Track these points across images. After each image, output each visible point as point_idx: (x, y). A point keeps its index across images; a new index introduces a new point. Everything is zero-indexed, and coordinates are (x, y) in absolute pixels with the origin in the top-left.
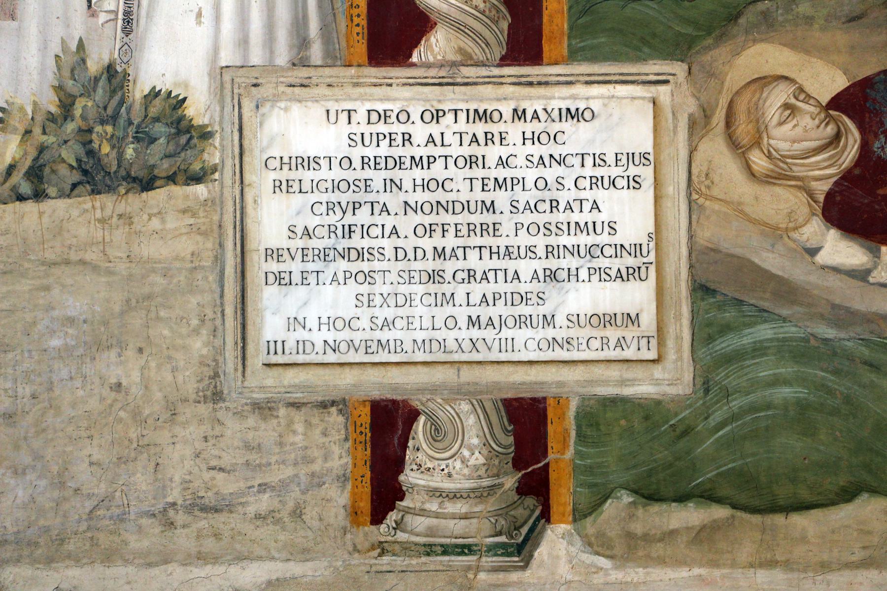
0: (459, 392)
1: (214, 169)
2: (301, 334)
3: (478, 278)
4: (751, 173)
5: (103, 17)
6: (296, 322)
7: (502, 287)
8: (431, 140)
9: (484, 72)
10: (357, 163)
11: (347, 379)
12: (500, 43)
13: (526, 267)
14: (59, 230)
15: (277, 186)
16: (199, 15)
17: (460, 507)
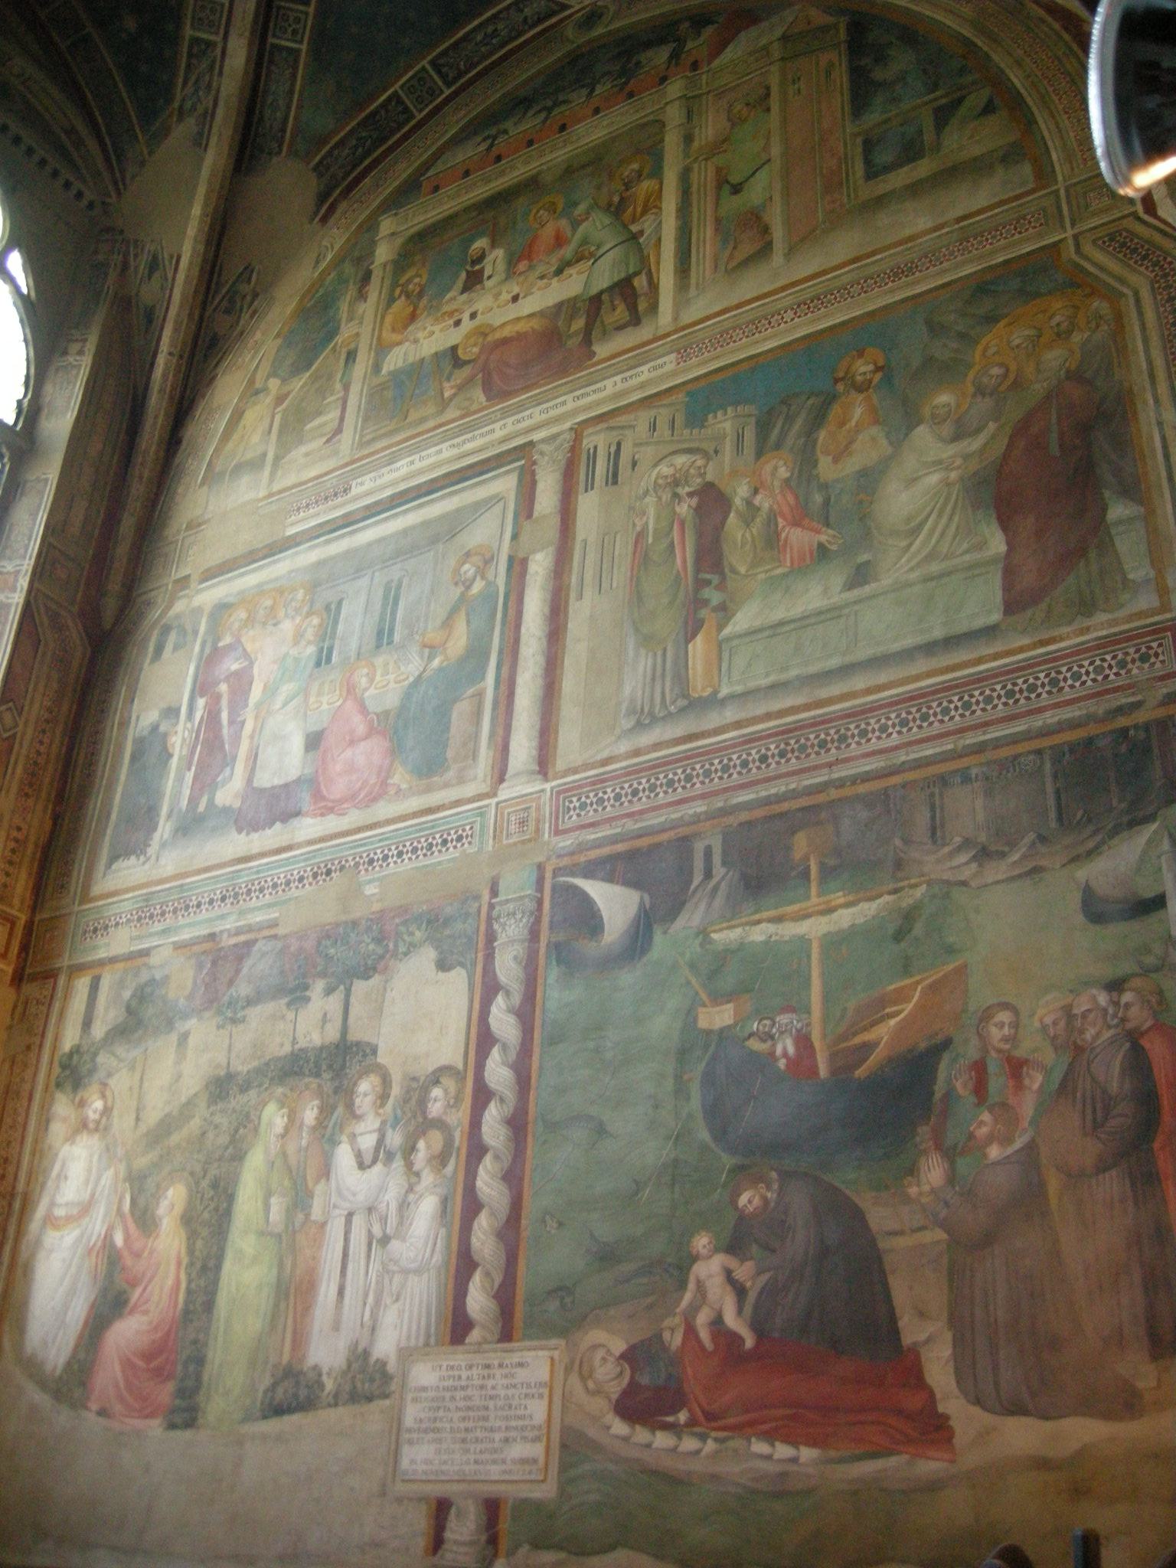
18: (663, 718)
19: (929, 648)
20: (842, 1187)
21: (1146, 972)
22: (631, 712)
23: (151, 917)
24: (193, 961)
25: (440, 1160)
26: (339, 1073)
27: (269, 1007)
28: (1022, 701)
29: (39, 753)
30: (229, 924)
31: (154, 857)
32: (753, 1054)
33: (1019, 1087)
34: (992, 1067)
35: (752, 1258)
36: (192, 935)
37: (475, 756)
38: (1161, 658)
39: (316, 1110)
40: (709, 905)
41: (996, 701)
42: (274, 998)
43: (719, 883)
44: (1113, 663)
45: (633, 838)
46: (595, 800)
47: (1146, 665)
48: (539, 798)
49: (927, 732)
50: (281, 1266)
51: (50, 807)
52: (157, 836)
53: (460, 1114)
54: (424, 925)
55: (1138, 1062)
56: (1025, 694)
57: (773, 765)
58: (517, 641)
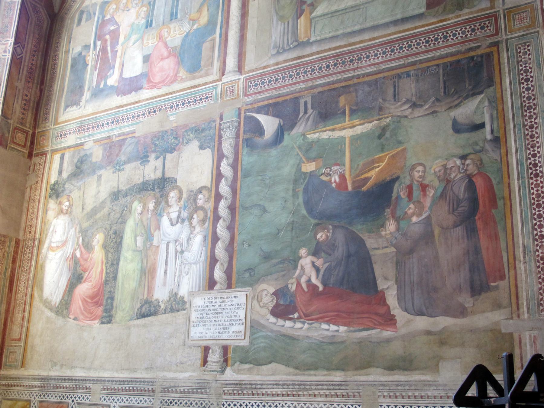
0: (217, 345)
2: (196, 335)
4: (260, 306)
6: (195, 333)
7: (223, 327)
8: (215, 302)
9: (223, 290)
11: (201, 342)
13: (227, 323)
17: (215, 364)
18: (288, 49)
19: (395, 23)
20: (356, 232)
21: (476, 152)
22: (275, 47)
23: (84, 130)
24: (102, 147)
25: (203, 221)
26: (162, 189)
27: (133, 165)
28: (432, 45)
29: (32, 64)
30: (116, 132)
31: (83, 106)
32: (322, 181)
33: (425, 195)
34: (415, 188)
35: (322, 258)
36: (101, 137)
37: (212, 64)
38: (489, 28)
39: (153, 204)
40: (306, 124)
41: (421, 45)
42: (135, 161)
43: (310, 115)
44: (470, 30)
45: (276, 98)
46: (261, 83)
47: (483, 31)
48: (238, 82)
49: (393, 57)
50: (142, 262)
51: (39, 86)
52: (84, 97)
53: (210, 204)
54: (194, 132)
55: (471, 186)
56: (433, 42)
57: (332, 69)
58: (228, 18)
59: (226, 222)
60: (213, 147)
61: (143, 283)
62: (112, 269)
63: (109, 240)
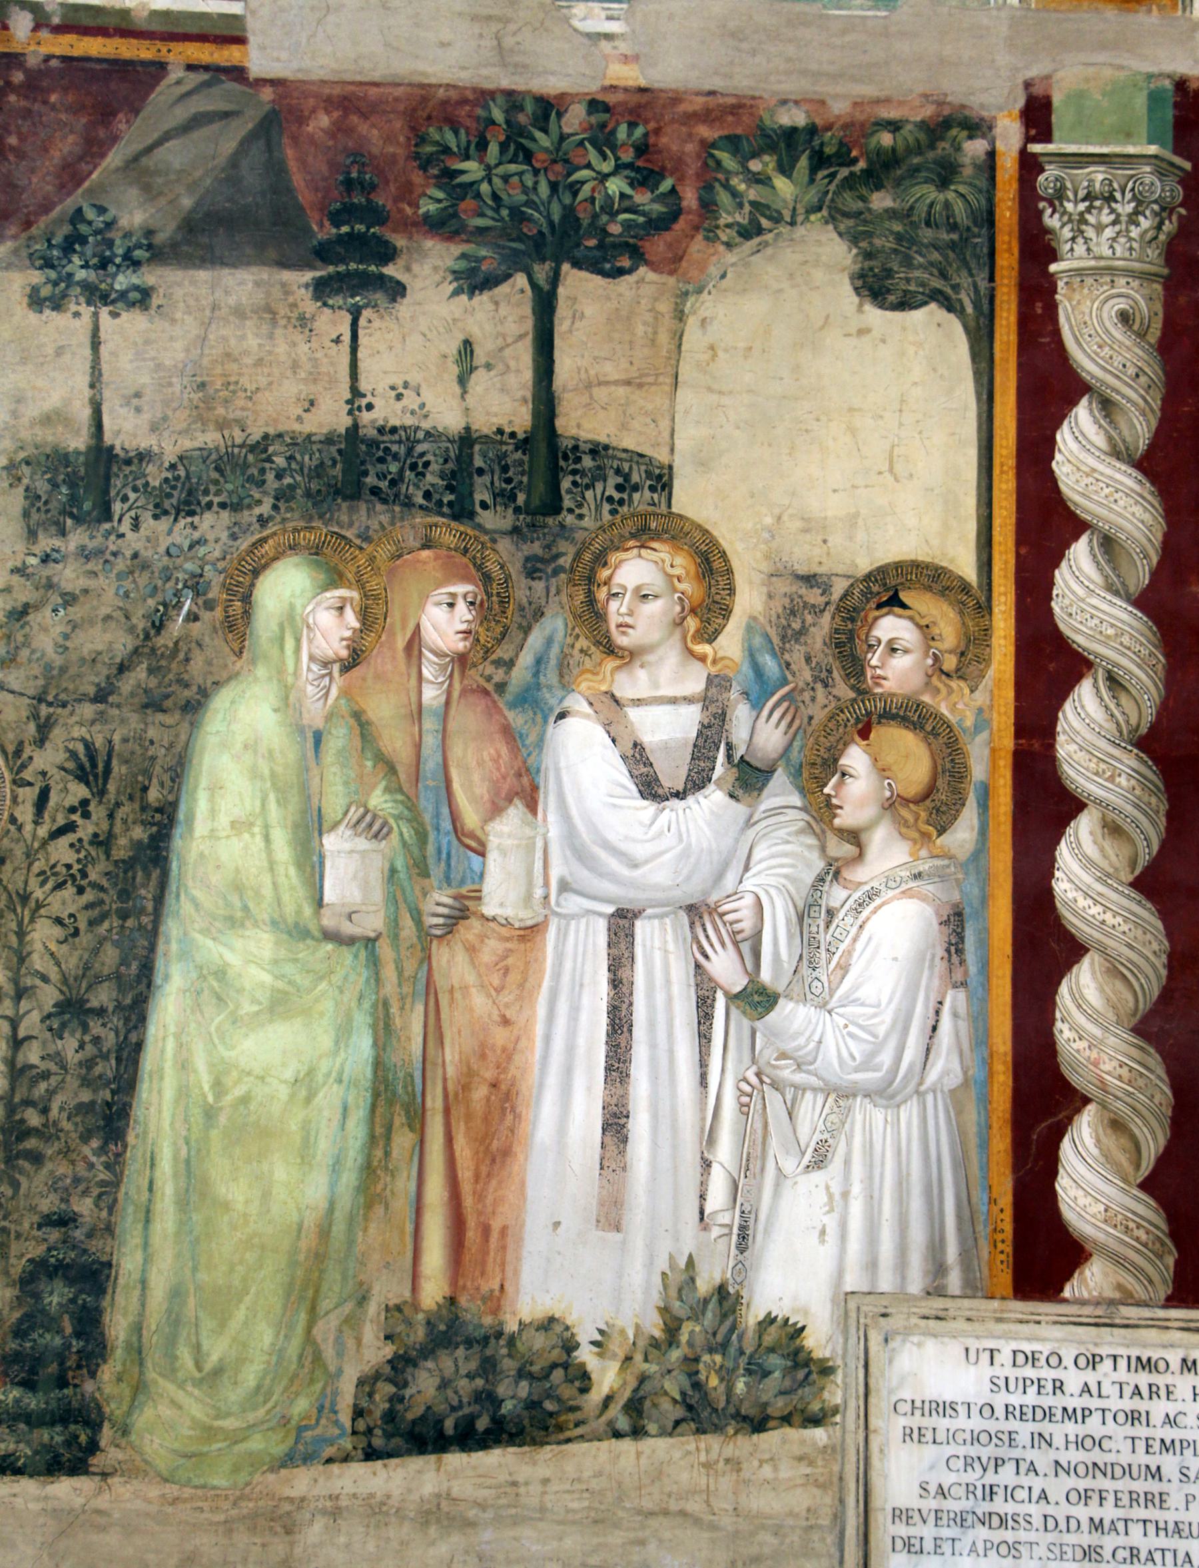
1: (835, 1411)
3: (1143, 1556)
5: (716, 1232)
8: (1086, 1389)
9: (1146, 1313)
10: (1000, 1412)
12: (1164, 1281)
14: (658, 1474)
15: (908, 1434)
16: (823, 1232)
53: (980, 698)
54: (803, 162)
59: (1130, 840)
60: (977, 305)
61: (405, 1184)
62: (69, 1046)
63: (26, 814)
